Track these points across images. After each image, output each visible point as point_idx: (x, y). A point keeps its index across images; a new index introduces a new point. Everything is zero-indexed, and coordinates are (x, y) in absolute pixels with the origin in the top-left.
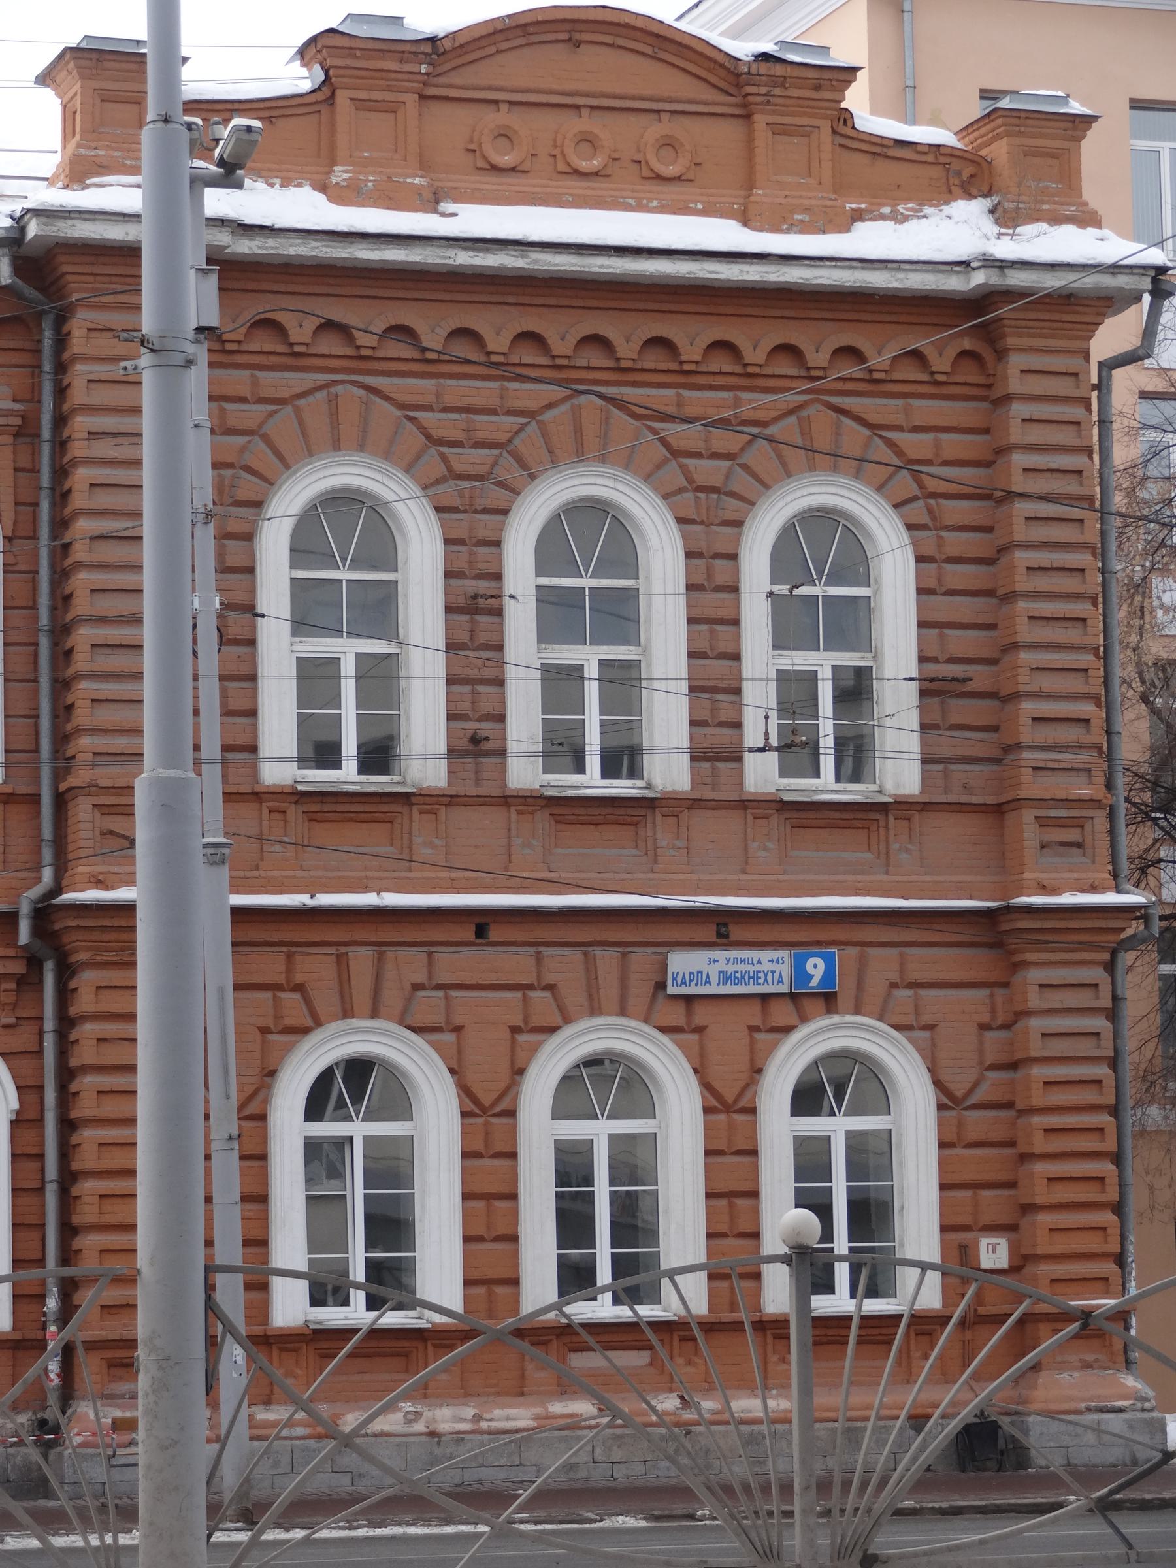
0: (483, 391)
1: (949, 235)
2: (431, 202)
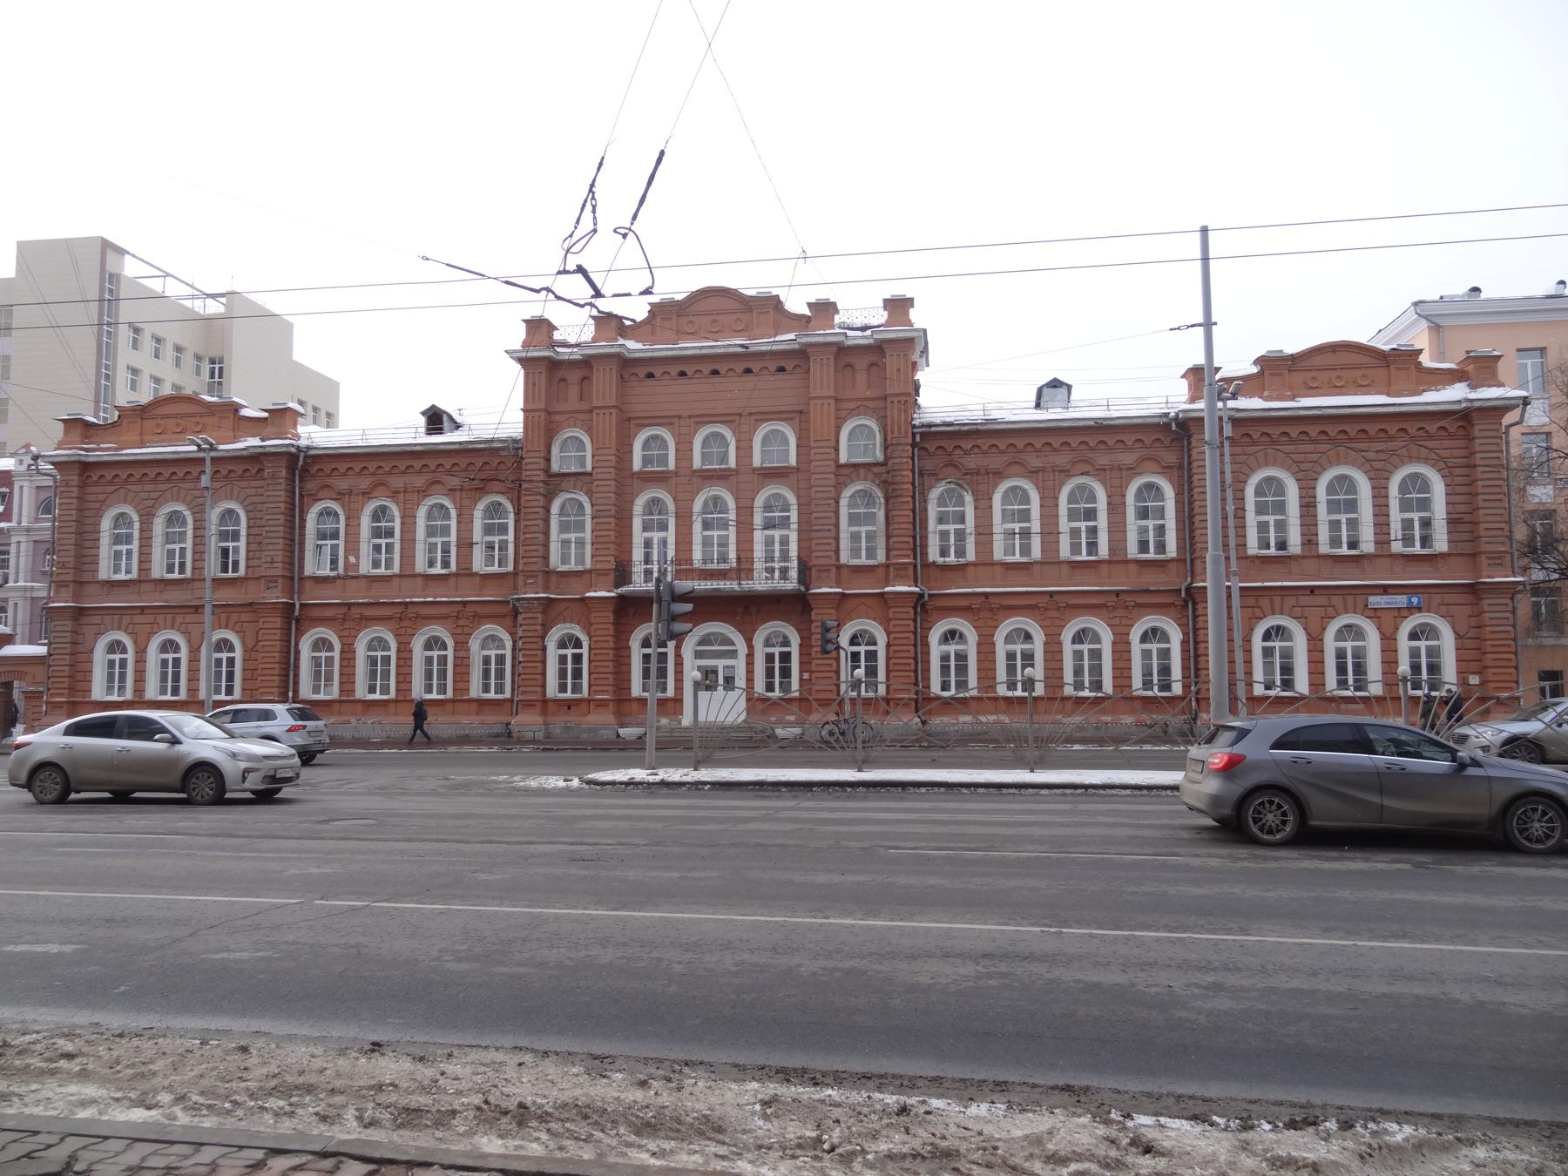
0: (1310, 447)
1: (1455, 394)
2: (1293, 399)
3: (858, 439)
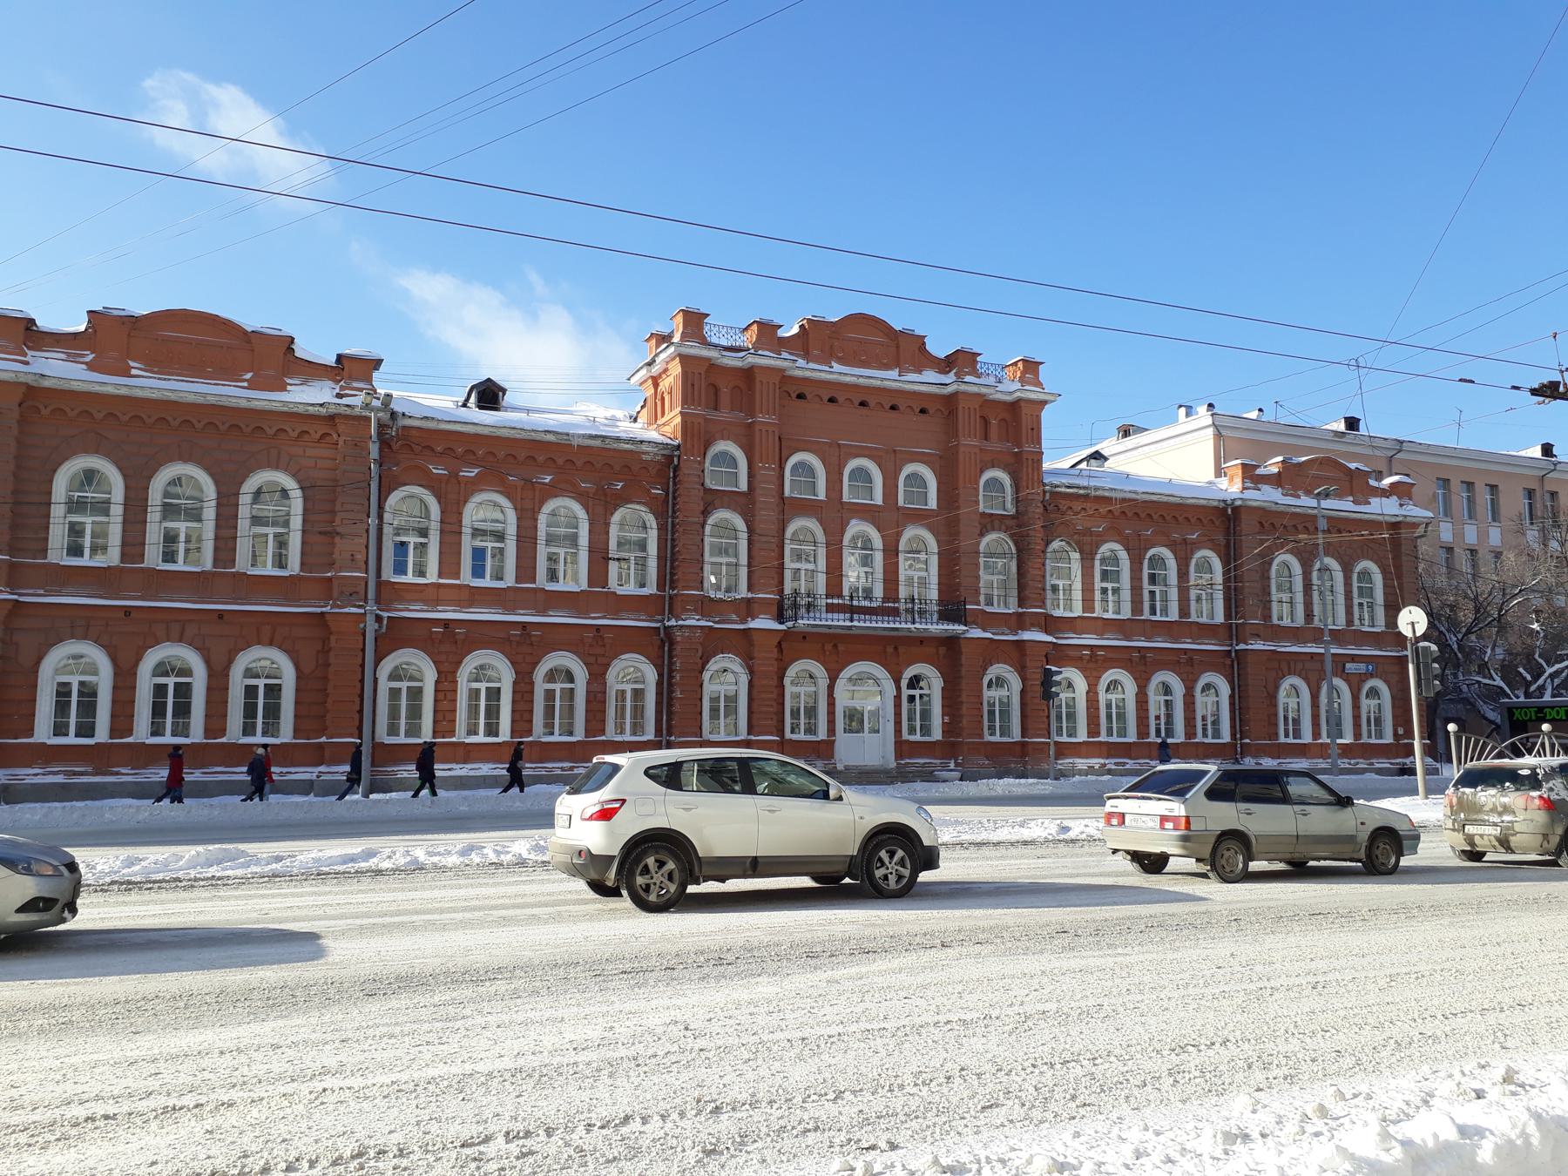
3: (994, 488)
